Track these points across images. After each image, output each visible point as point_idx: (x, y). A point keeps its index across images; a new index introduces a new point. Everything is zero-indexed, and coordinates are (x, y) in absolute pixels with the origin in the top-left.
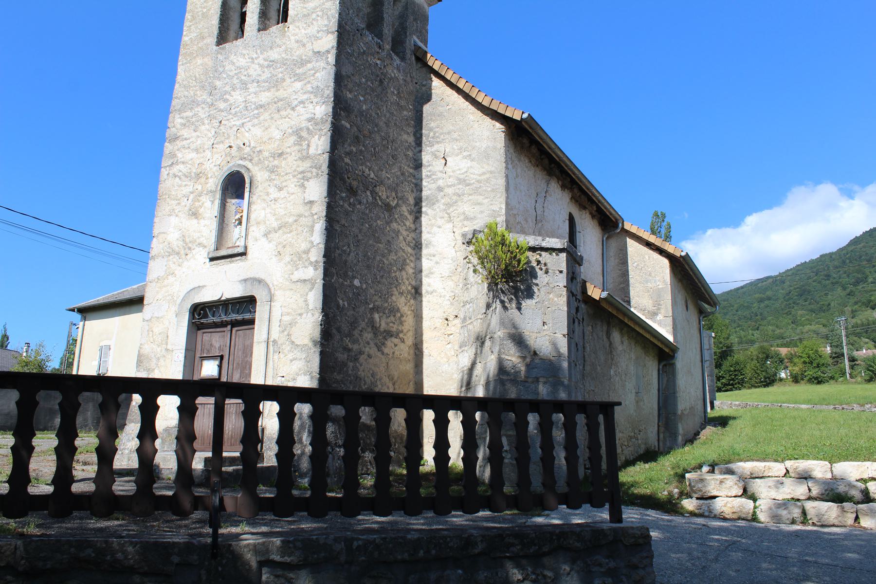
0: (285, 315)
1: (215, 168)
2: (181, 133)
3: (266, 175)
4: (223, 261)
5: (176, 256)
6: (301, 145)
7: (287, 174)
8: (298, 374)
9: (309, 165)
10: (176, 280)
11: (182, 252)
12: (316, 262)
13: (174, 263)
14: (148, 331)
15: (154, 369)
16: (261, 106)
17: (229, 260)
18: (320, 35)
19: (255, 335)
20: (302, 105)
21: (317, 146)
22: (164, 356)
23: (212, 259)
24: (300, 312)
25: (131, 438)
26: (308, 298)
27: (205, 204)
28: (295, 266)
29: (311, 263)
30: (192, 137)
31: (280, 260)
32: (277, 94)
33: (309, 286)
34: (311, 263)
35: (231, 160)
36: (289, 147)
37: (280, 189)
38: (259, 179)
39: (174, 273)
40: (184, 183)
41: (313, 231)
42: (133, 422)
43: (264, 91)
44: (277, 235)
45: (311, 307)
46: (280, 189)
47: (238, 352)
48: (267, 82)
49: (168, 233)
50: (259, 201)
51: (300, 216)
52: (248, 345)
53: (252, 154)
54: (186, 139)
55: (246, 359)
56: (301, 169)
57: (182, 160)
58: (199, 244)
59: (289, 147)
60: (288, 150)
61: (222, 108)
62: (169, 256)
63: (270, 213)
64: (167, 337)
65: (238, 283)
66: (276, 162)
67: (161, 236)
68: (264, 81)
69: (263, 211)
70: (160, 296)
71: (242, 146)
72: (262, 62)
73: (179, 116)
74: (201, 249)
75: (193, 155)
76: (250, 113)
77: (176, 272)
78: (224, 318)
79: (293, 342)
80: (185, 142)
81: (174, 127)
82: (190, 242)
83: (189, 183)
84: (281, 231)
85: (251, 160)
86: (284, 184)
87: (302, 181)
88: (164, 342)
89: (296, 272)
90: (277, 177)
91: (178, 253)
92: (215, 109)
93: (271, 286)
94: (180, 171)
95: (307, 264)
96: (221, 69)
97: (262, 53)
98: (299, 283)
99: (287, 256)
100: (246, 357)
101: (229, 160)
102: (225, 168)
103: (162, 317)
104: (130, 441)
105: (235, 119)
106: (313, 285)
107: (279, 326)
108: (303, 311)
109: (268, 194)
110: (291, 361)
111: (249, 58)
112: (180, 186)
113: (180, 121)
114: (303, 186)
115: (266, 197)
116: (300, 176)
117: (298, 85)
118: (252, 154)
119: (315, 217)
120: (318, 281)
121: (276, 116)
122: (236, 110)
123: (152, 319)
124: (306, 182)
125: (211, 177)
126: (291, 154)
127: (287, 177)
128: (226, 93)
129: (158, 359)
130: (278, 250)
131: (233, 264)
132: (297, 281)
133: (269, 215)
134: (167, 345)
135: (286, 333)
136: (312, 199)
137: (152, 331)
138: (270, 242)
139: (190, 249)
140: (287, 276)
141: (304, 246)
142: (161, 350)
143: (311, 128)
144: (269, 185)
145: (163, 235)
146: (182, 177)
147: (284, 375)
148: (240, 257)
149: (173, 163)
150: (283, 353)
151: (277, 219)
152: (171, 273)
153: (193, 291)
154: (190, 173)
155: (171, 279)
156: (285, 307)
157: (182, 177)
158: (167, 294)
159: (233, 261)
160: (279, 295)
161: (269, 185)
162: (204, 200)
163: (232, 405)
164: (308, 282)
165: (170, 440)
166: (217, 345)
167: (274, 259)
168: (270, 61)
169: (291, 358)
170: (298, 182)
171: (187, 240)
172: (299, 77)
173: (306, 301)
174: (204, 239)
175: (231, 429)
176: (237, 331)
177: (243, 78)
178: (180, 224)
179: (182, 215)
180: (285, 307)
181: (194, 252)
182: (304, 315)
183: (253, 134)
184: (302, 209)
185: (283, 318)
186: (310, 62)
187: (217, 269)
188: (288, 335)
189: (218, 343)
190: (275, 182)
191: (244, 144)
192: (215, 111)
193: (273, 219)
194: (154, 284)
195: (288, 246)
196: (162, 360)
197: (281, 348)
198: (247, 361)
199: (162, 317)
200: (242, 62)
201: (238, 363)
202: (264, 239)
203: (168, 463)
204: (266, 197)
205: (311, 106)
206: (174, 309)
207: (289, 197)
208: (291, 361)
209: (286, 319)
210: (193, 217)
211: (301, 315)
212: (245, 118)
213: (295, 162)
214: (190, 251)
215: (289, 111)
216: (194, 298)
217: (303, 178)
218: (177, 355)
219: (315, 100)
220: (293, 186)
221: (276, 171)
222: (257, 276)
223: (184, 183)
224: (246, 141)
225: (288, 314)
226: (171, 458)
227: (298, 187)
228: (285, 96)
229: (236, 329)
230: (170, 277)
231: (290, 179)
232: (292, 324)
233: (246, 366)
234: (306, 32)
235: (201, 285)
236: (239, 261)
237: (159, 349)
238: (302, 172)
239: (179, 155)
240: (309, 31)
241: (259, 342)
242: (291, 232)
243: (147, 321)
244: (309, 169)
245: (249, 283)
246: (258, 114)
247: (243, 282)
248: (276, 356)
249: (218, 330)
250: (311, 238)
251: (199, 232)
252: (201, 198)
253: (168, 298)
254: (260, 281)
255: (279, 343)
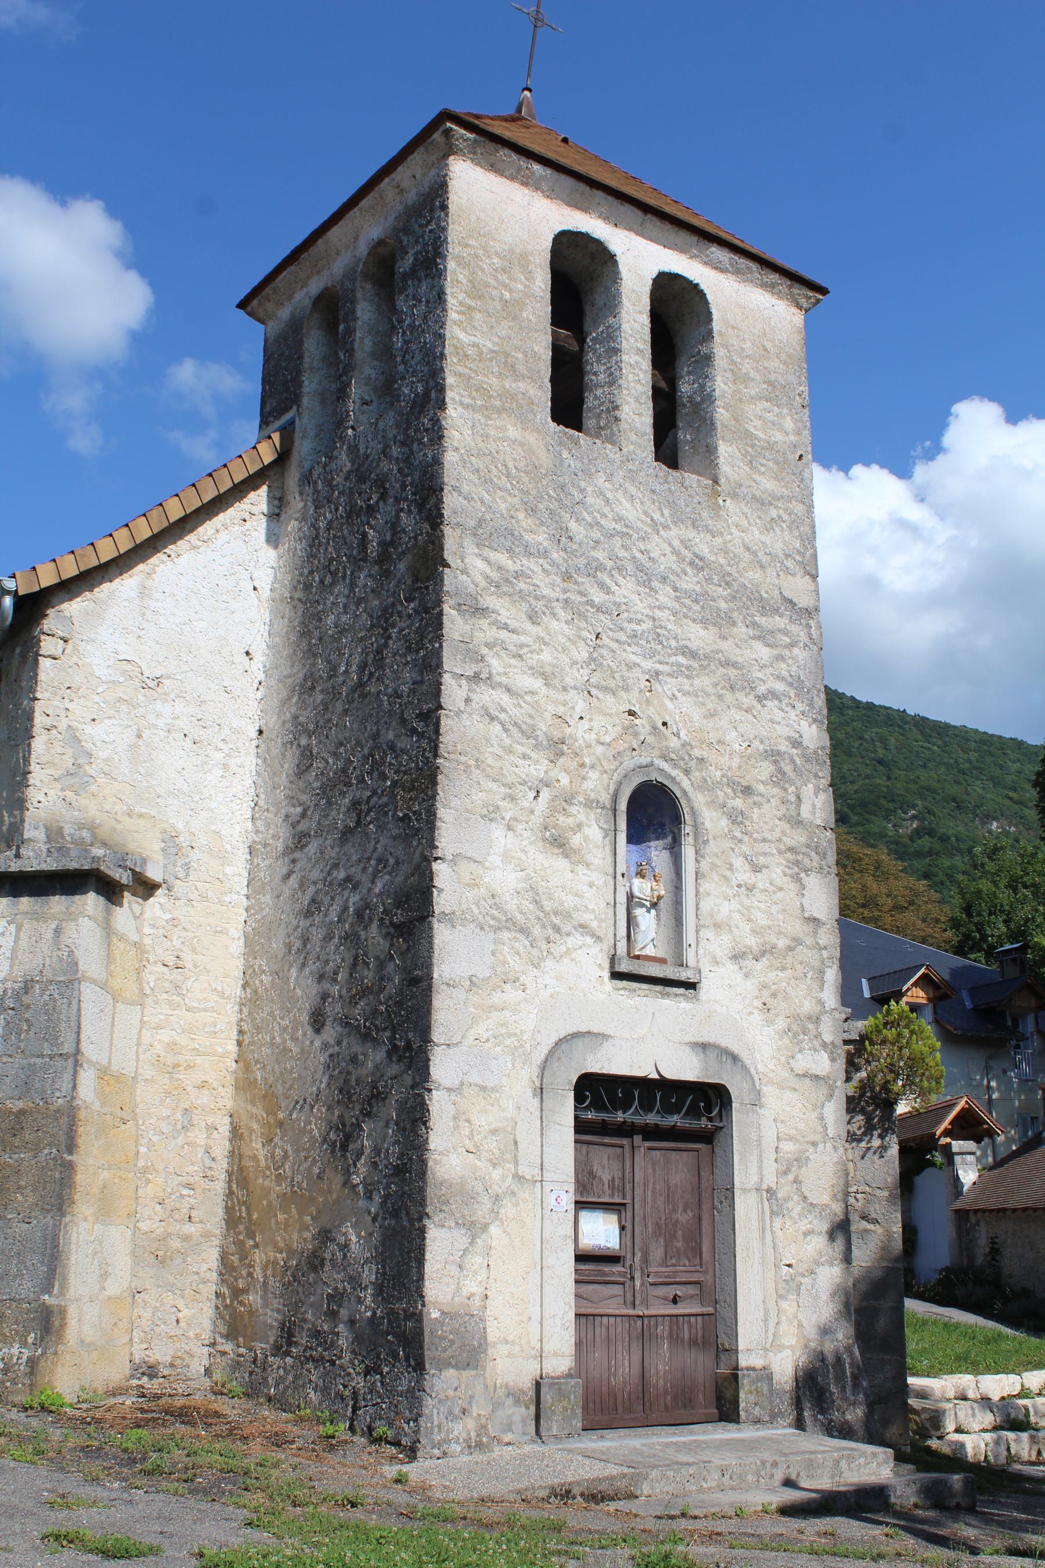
0: (786, 1140)
1: (600, 750)
2: (490, 601)
3: (724, 822)
4: (644, 986)
5: (522, 937)
6: (786, 790)
7: (764, 840)
8: (817, 1263)
9: (803, 840)
10: (526, 1000)
11: (537, 931)
12: (833, 1043)
13: (518, 954)
14: (455, 1118)
15: (485, 1227)
16: (693, 655)
17: (659, 988)
18: (789, 563)
19: (736, 1172)
20: (776, 702)
21: (814, 806)
22: (513, 1193)
23: (616, 975)
24: (812, 1137)
25: (457, 1411)
26: (825, 1115)
27: (587, 830)
28: (798, 1044)
29: (824, 1045)
30: (524, 632)
31: (769, 1022)
32: (725, 645)
33: (825, 1090)
34: (824, 1045)
35: (639, 746)
36: (762, 782)
37: (756, 869)
38: (708, 824)
39: (518, 979)
40: (520, 749)
41: (822, 982)
42: (448, 1365)
43: (694, 621)
44: (758, 966)
45: (831, 1132)
46: (756, 869)
47: (654, 1199)
48: (696, 601)
49: (487, 864)
50: (716, 878)
51: (798, 941)
52: (676, 1186)
53: (686, 758)
54: (506, 627)
55: (674, 1217)
56: (788, 842)
57: (504, 680)
58: (582, 926)
59: (762, 782)
60: (761, 788)
61: (597, 600)
62: (499, 929)
63: (739, 912)
64: (516, 1143)
65: (688, 1049)
66: (738, 803)
67: (463, 866)
68: (688, 594)
69: (726, 903)
70: (481, 1030)
71: (660, 725)
72: (676, 543)
73: (476, 551)
74: (589, 940)
75: (537, 684)
76: (669, 656)
77: (523, 978)
78: (639, 1120)
79: (805, 1197)
80: (504, 634)
81: (464, 571)
82: (556, 913)
83: (533, 755)
84: (764, 961)
85: (687, 772)
86: (762, 860)
87: (796, 869)
88: (508, 1156)
89: (799, 1056)
90: (746, 839)
91: (524, 931)
92: (581, 593)
93: (753, 1071)
94: (503, 710)
95: (816, 1043)
96: (578, 497)
97: (675, 523)
98: (807, 1081)
99: (781, 1017)
100: (674, 1210)
101: (635, 747)
102: (629, 763)
103: (494, 1089)
104: (456, 1418)
105: (635, 649)
106: (832, 1088)
107: (776, 1161)
108: (818, 1138)
109: (731, 867)
110: (806, 1234)
111: (645, 513)
112: (510, 751)
113: (481, 565)
114: (796, 879)
115: (728, 874)
116: (788, 855)
117: (764, 653)
118: (686, 758)
119: (825, 953)
120: (839, 1083)
121: (729, 697)
122: (634, 626)
123: (466, 1089)
124: (803, 875)
125: (593, 767)
126: (769, 801)
127: (765, 847)
128: (601, 568)
129: (497, 1198)
130: (764, 1000)
131: (667, 1002)
132: (804, 1076)
133: (736, 915)
134: (516, 1162)
135: (791, 1177)
136: (816, 915)
137: (468, 1121)
138: (746, 976)
139: (557, 929)
140: (783, 1059)
141: (808, 1006)
142: (504, 1178)
143: (798, 761)
144: (733, 850)
145: (473, 865)
146: (511, 727)
147: (793, 1262)
148: (681, 991)
149: (476, 677)
150: (791, 1217)
151: (753, 931)
152: (511, 976)
153: (579, 1043)
154: (534, 729)
155: (511, 994)
156: (782, 1122)
157: (511, 727)
158: (503, 1031)
159: (668, 995)
160: (769, 1092)
161: (733, 850)
162: (582, 817)
163: (660, 1319)
164: (822, 1082)
165: (565, 1409)
166: (606, 1177)
167: (757, 1017)
168: (697, 556)
169: (804, 1228)
170: (789, 868)
171: (548, 905)
172: (764, 636)
173: (821, 1118)
174: (592, 917)
175: (662, 1373)
176: (650, 1149)
177: (639, 555)
178: (524, 857)
179: (525, 834)
180: (782, 1122)
181: (571, 941)
182: (821, 1146)
183: (683, 710)
184: (797, 927)
185: (781, 1146)
186: (776, 611)
187: (632, 1002)
188: (796, 1181)
189: (606, 1171)
190: (744, 848)
191: (665, 724)
192: (579, 598)
193: (748, 928)
194: (460, 994)
195: (780, 996)
196: (507, 1202)
197: (786, 1205)
198: (677, 1220)
199: (494, 1089)
200: (630, 512)
201: (657, 1224)
202: (731, 967)
203: (819, 1471)
204: (728, 874)
205: (792, 714)
206: (527, 1075)
207: (774, 892)
208: (806, 1234)
209: (788, 1147)
210: (556, 851)
211: (814, 1144)
212: (661, 663)
213: (777, 822)
214: (557, 936)
215: (749, 701)
216: (585, 1059)
217: (797, 863)
218: (554, 1196)
219: (801, 706)
220: (778, 871)
221: (742, 823)
222: (723, 1043)
223: (520, 749)
224: (667, 719)
225: (791, 1138)
226: (824, 1459)
227: (789, 879)
228: (740, 660)
229: (648, 1144)
230: (508, 987)
231: (772, 855)
232: (800, 1160)
233: (675, 1232)
234: (763, 538)
235: (595, 1029)
236: (681, 999)
237: (496, 1174)
238: (791, 850)
239: (495, 664)
240: (767, 539)
241: (745, 1191)
242: (783, 969)
243: (449, 1090)
244: (804, 850)
245: (712, 1055)
246: (688, 668)
247: (700, 1050)
248: (778, 1223)
249: (607, 1140)
250: (821, 995)
251: (577, 895)
252: (574, 809)
253: (508, 1042)
254: (735, 1058)
255: (779, 1195)
